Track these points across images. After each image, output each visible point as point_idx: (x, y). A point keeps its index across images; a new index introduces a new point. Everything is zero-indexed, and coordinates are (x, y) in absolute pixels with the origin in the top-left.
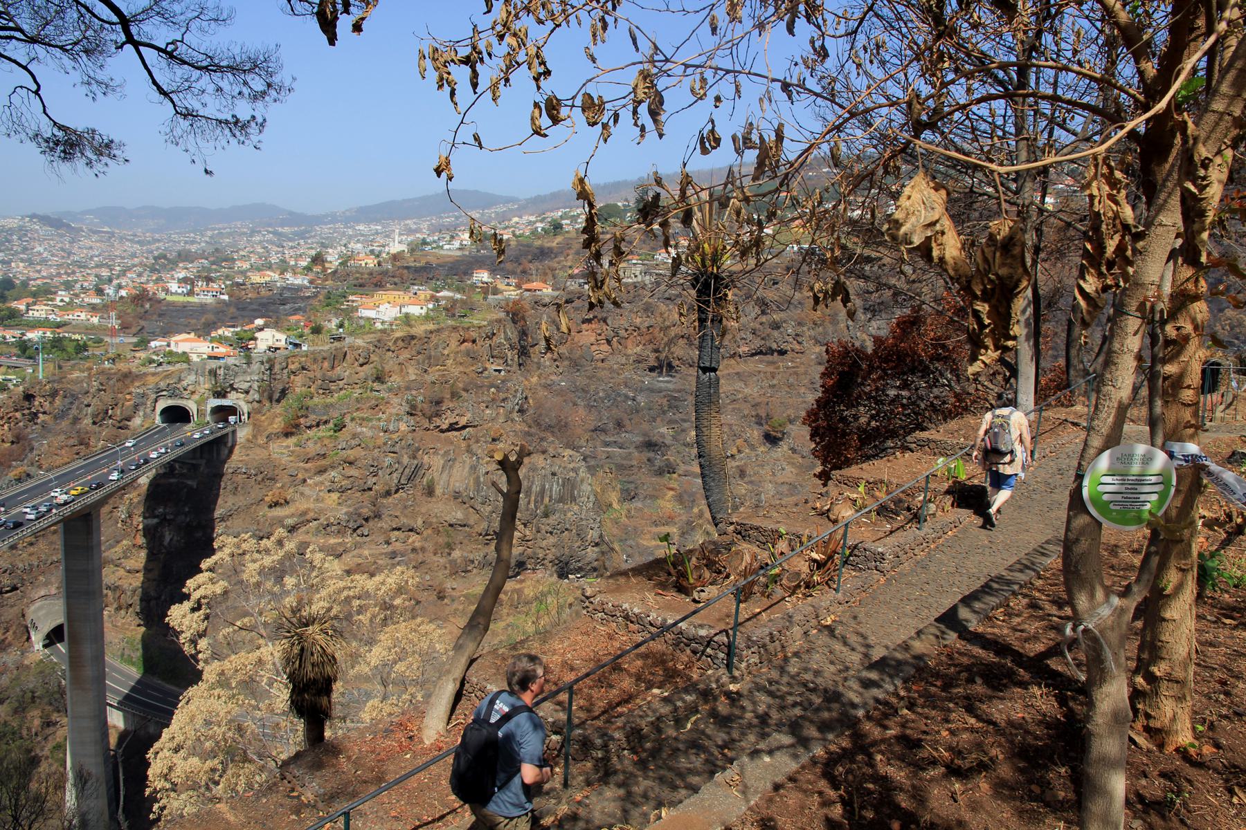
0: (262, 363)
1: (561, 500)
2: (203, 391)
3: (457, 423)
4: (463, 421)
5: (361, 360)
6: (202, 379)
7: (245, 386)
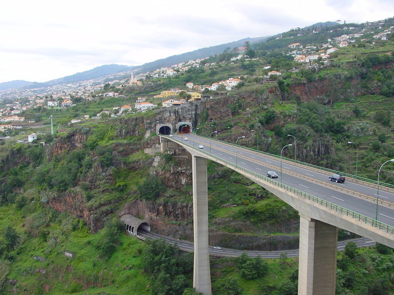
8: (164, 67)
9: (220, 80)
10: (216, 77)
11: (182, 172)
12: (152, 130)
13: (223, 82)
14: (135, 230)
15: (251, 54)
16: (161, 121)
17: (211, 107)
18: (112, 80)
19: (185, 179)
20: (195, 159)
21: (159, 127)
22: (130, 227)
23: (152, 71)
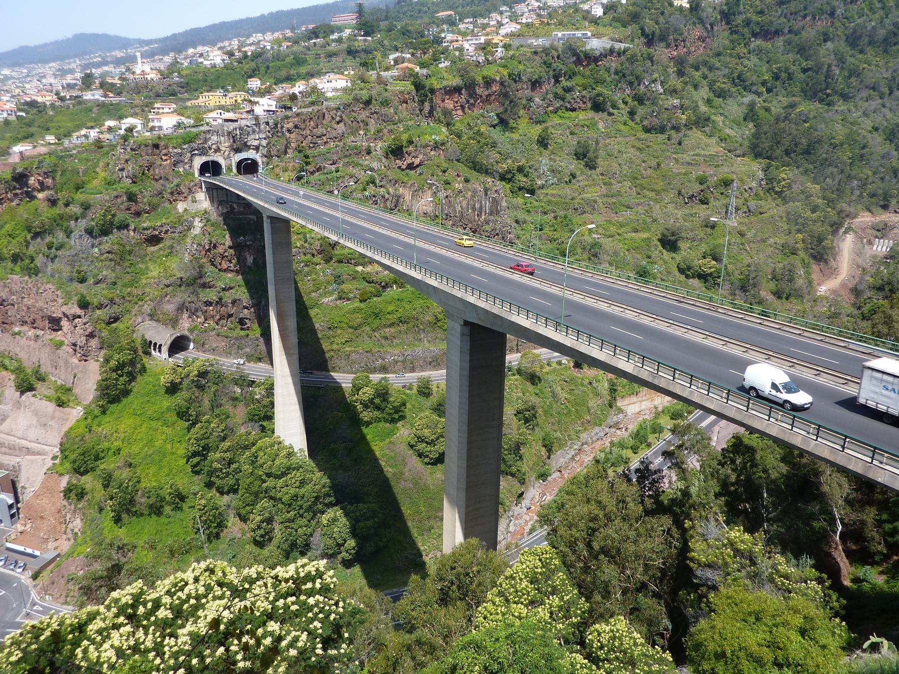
0: (267, 123)
1: (491, 214)
2: (224, 149)
3: (413, 163)
4: (417, 161)
5: (338, 119)
6: (222, 139)
7: (256, 143)
8: (204, 45)
9: (312, 75)
10: (303, 70)
11: (246, 245)
12: (187, 167)
13: (317, 81)
14: (165, 349)
15: (366, 27)
16: (204, 152)
17: (296, 127)
18: (99, 65)
19: (252, 257)
20: (269, 220)
21: (198, 162)
22: (155, 344)
23: (180, 52)
